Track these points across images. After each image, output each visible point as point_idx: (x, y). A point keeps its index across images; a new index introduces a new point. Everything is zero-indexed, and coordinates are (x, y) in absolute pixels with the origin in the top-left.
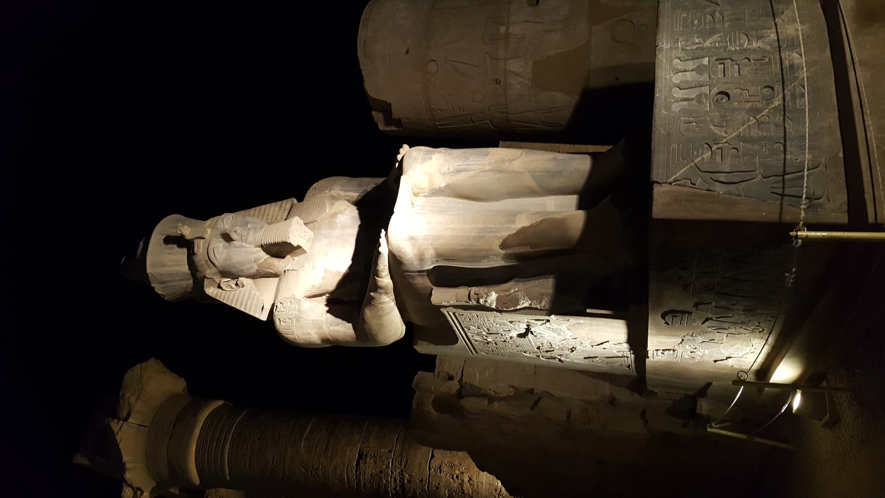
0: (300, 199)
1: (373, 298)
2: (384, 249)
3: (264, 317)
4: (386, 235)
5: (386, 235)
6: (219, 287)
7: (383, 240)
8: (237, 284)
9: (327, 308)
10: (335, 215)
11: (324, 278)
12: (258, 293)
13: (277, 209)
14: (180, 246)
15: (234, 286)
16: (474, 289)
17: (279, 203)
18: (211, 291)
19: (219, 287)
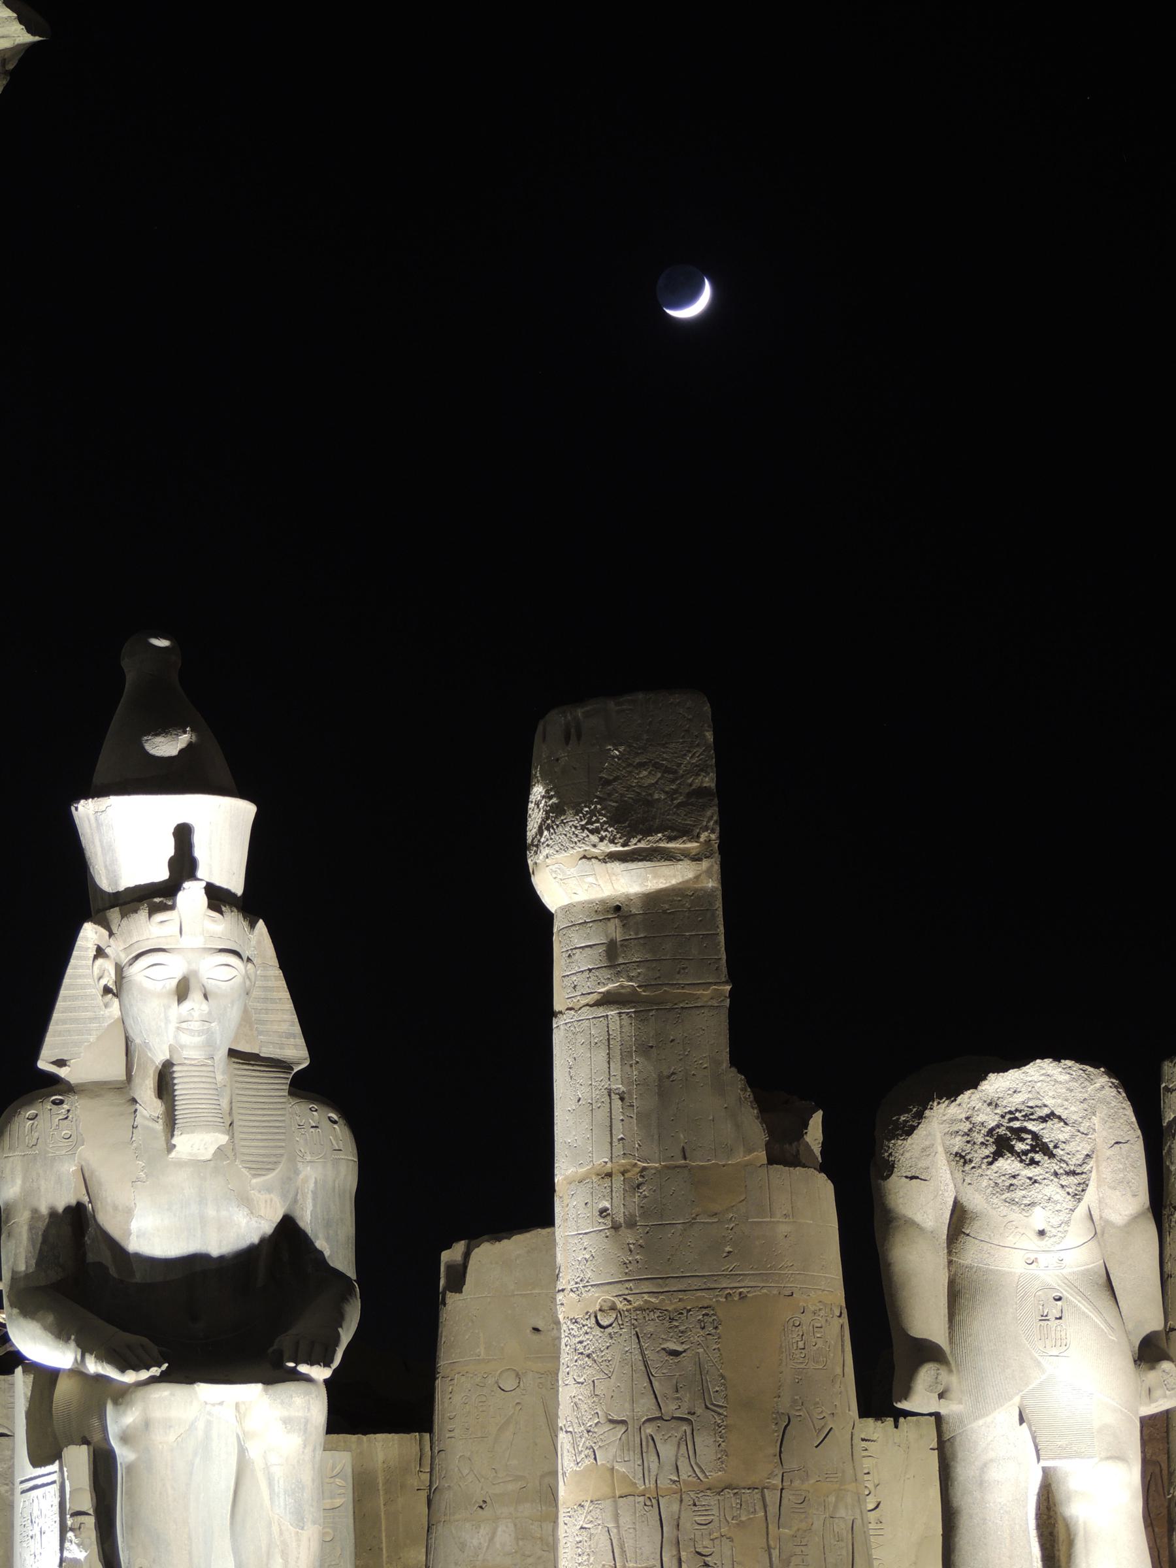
0: (304, 1086)
1: (69, 1339)
2: (130, 1377)
3: (42, 1065)
4: (153, 1380)
5: (153, 1380)
6: (100, 953)
7: (144, 1375)
8: (107, 990)
9: (60, 1210)
10: (245, 1201)
11: (116, 1208)
12: (92, 1039)
13: (285, 1027)
14: (173, 864)
15: (103, 982)
16: (90, 1521)
17: (297, 1029)
18: (90, 934)
19: (100, 953)
